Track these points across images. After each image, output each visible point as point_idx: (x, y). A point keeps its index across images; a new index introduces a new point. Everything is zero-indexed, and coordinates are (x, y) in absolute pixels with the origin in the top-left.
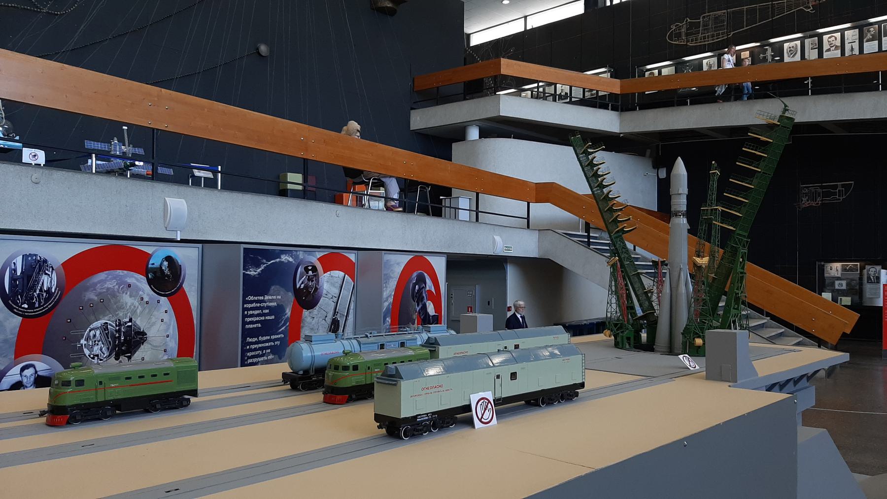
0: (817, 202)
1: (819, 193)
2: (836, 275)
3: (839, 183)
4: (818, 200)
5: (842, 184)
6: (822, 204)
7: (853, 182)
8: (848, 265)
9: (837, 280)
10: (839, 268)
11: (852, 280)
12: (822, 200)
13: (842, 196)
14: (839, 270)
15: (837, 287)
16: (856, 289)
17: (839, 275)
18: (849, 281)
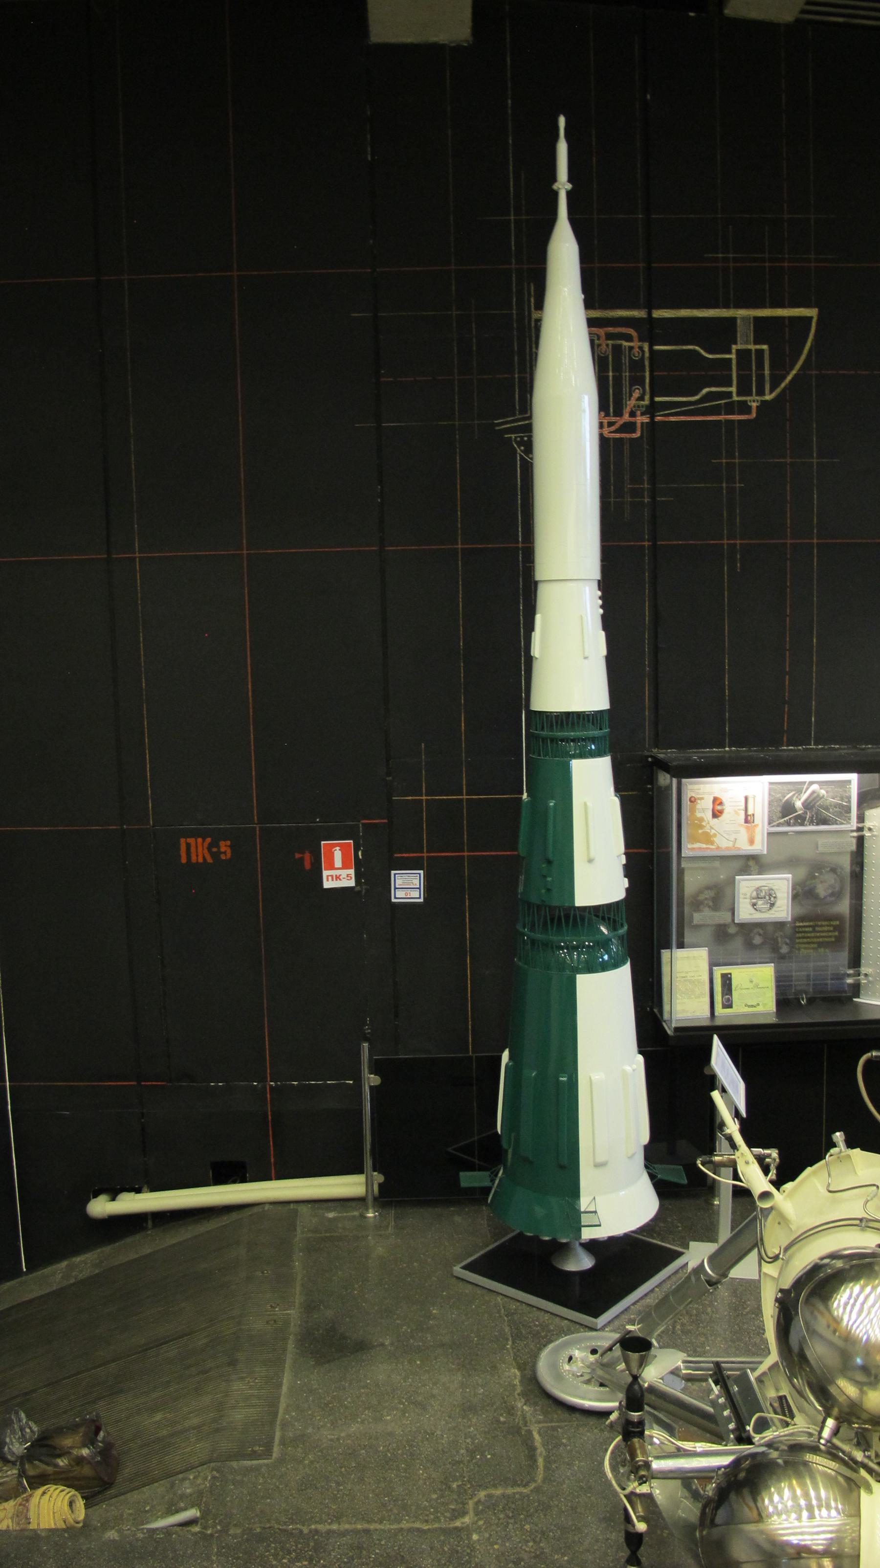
0: (626, 417)
1: (636, 366)
2: (744, 847)
3: (741, 313)
4: (632, 403)
5: (756, 319)
6: (652, 426)
7: (812, 312)
8: (798, 788)
9: (745, 870)
10: (760, 810)
11: (817, 867)
12: (652, 410)
13: (761, 392)
14: (758, 820)
15: (745, 913)
16: (839, 917)
17: (760, 846)
18: (802, 872)
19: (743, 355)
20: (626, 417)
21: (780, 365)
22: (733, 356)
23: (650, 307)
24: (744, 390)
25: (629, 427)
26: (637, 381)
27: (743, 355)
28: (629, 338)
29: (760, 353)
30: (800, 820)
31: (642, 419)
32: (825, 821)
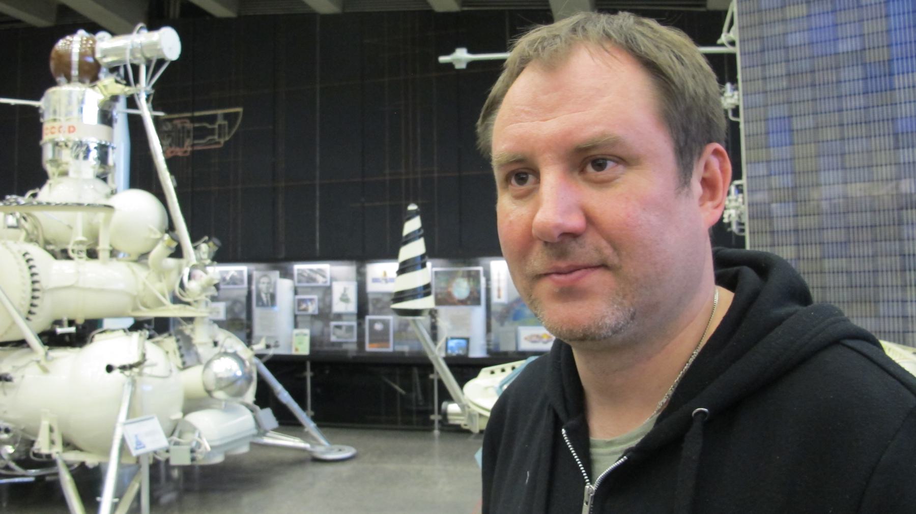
0: (185, 149)
6: (193, 152)
7: (239, 110)
8: (227, 272)
11: (235, 302)
12: (193, 145)
18: (229, 303)
19: (220, 126)
20: (185, 149)
21: (231, 126)
22: (216, 126)
23: (193, 110)
24: (220, 136)
25: (185, 152)
26: (188, 136)
27: (220, 126)
28: (185, 122)
29: (224, 125)
30: (228, 284)
31: (190, 149)
32: (235, 283)
